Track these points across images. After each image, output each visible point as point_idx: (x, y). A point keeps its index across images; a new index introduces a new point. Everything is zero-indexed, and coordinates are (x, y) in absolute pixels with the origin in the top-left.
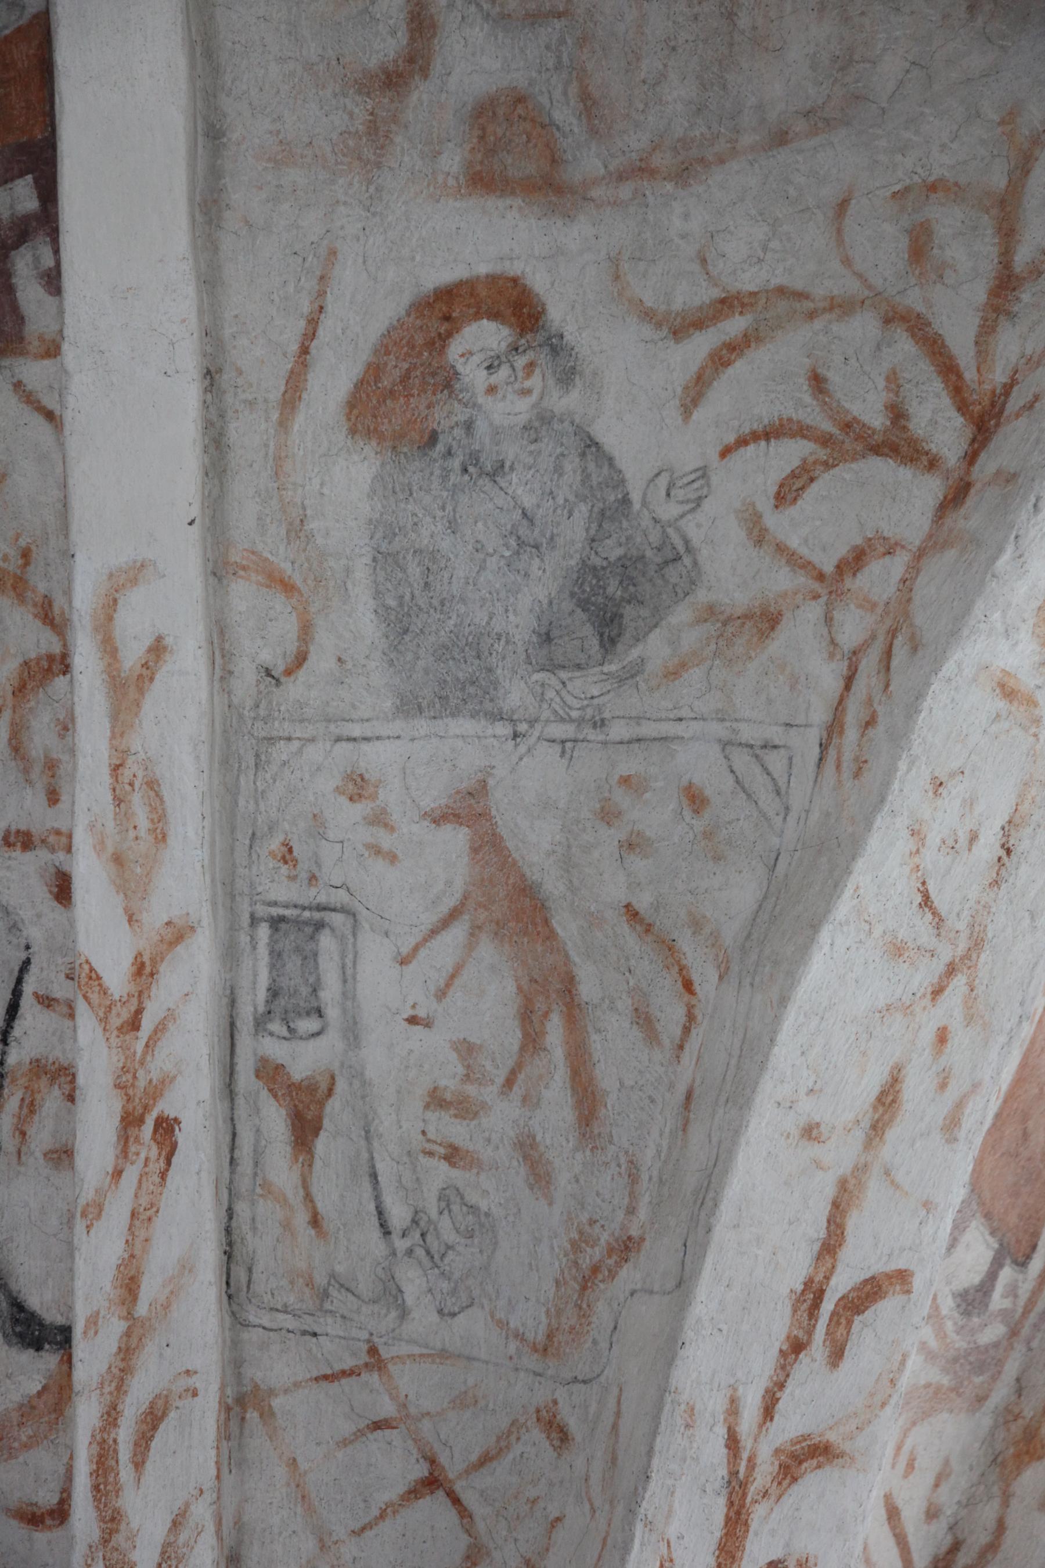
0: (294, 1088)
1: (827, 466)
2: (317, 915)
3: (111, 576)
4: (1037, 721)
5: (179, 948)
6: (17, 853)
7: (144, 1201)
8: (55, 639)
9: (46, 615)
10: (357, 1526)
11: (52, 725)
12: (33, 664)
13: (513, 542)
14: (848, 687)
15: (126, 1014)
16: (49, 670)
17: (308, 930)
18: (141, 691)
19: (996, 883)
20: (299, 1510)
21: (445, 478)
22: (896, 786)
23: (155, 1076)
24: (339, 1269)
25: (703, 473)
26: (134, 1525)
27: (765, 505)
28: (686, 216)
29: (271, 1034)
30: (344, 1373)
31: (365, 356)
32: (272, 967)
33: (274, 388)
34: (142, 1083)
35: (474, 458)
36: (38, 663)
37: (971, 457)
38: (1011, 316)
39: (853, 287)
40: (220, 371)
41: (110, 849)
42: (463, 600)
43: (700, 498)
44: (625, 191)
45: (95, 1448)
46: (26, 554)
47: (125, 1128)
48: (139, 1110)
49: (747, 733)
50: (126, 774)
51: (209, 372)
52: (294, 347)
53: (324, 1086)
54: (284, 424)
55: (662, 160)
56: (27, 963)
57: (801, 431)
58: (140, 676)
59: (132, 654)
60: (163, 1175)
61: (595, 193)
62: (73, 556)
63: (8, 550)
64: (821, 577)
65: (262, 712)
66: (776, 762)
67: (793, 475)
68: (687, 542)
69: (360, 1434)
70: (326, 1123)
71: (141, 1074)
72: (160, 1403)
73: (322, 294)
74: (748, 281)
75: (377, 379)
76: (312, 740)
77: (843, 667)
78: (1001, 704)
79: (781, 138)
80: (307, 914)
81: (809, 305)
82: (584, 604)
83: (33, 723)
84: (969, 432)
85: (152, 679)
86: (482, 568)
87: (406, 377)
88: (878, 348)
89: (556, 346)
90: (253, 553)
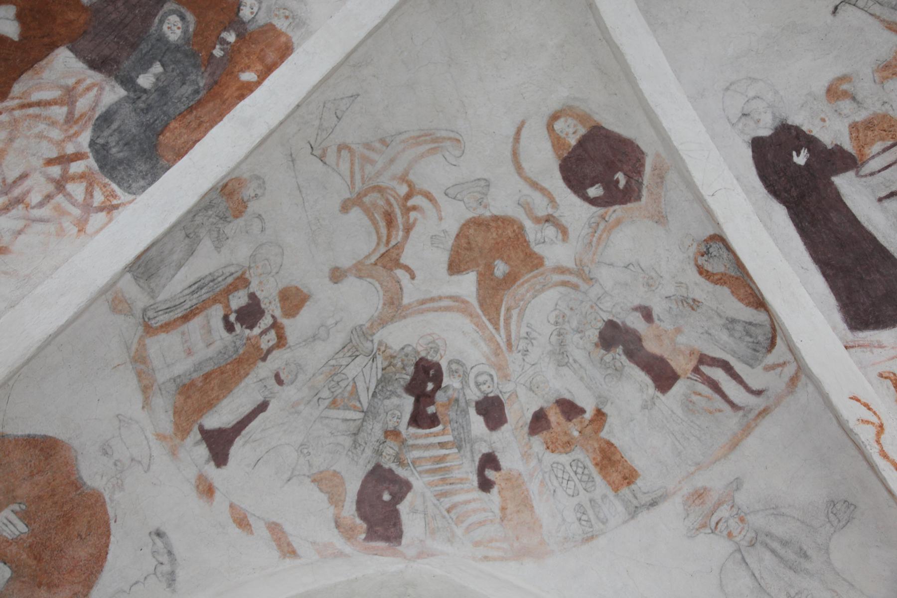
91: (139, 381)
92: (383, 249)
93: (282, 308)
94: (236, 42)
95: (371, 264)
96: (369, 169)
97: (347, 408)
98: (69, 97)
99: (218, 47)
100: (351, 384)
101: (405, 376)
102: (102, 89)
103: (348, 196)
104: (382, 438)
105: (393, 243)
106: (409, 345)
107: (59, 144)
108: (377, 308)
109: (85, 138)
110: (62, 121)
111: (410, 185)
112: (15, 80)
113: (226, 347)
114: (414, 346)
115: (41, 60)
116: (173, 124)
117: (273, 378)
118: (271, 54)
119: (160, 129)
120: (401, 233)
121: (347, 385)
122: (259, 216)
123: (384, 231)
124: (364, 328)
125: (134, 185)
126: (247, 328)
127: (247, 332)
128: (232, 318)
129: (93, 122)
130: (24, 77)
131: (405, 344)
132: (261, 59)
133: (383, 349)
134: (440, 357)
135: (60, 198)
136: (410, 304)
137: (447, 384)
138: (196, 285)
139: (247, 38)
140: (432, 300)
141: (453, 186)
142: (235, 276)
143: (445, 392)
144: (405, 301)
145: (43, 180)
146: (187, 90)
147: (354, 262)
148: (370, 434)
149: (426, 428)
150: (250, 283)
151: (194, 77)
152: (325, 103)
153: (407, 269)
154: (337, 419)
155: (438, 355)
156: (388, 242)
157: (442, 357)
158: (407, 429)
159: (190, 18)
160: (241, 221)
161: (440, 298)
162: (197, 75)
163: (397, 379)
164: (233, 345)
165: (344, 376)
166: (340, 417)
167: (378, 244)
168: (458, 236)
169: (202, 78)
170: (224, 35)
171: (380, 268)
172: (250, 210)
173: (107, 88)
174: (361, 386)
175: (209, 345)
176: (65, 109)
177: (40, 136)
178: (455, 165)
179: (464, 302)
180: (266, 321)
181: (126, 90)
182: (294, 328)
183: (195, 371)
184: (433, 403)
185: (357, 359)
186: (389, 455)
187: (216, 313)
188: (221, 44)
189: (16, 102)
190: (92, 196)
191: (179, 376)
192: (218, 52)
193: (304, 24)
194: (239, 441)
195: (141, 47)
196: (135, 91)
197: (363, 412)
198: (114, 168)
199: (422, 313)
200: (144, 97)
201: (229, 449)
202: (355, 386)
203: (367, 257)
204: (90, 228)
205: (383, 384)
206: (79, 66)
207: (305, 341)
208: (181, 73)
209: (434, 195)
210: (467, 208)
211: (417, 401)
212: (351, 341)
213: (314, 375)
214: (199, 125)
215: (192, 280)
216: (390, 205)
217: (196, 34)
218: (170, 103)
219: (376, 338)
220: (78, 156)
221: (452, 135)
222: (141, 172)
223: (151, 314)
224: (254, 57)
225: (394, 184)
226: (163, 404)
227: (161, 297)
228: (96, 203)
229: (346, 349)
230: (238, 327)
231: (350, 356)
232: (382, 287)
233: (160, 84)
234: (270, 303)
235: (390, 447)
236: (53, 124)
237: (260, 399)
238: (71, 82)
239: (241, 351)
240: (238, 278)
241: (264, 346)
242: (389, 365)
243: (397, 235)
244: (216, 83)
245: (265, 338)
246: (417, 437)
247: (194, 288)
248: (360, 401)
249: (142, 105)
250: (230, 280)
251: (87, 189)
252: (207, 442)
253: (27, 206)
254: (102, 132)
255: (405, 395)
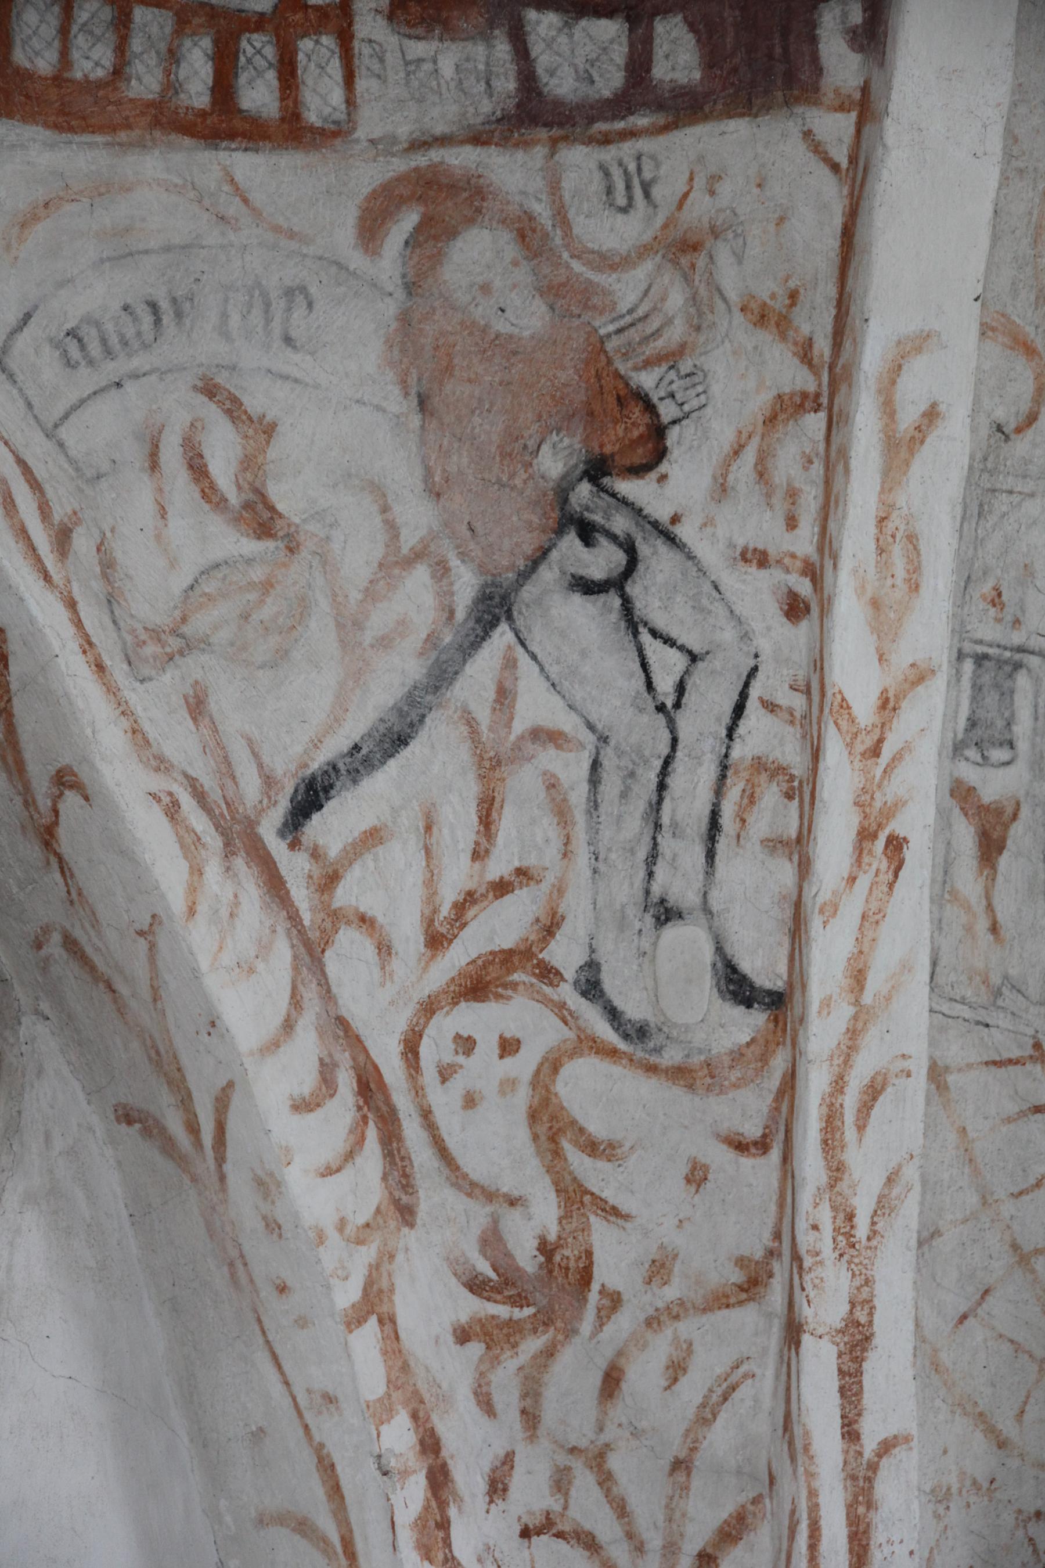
0: (983, 809)
2: (1018, 657)
3: (899, 342)
5: (920, 689)
6: (753, 569)
7: (874, 906)
8: (811, 378)
9: (805, 355)
10: (1016, 1190)
11: (798, 457)
12: (786, 398)
15: (869, 741)
16: (801, 406)
17: (1008, 669)
18: (912, 452)
20: (967, 1170)
23: (890, 799)
24: (1013, 972)
26: (856, 1176)
29: (967, 759)
30: (1010, 1062)
32: (974, 699)
34: (878, 804)
36: (791, 398)
41: (869, 594)
45: (825, 1110)
46: (793, 296)
47: (860, 841)
48: (874, 827)
50: (890, 526)
53: (1009, 811)
56: (755, 669)
58: (913, 438)
59: (908, 417)
60: (891, 886)
62: (866, 320)
63: (776, 289)
65: (990, 465)
69: (1022, 1114)
70: (1009, 843)
71: (878, 795)
72: (880, 1078)
76: (1032, 495)
80: (1008, 654)
83: (780, 452)
85: (922, 442)
90: (1003, 315)
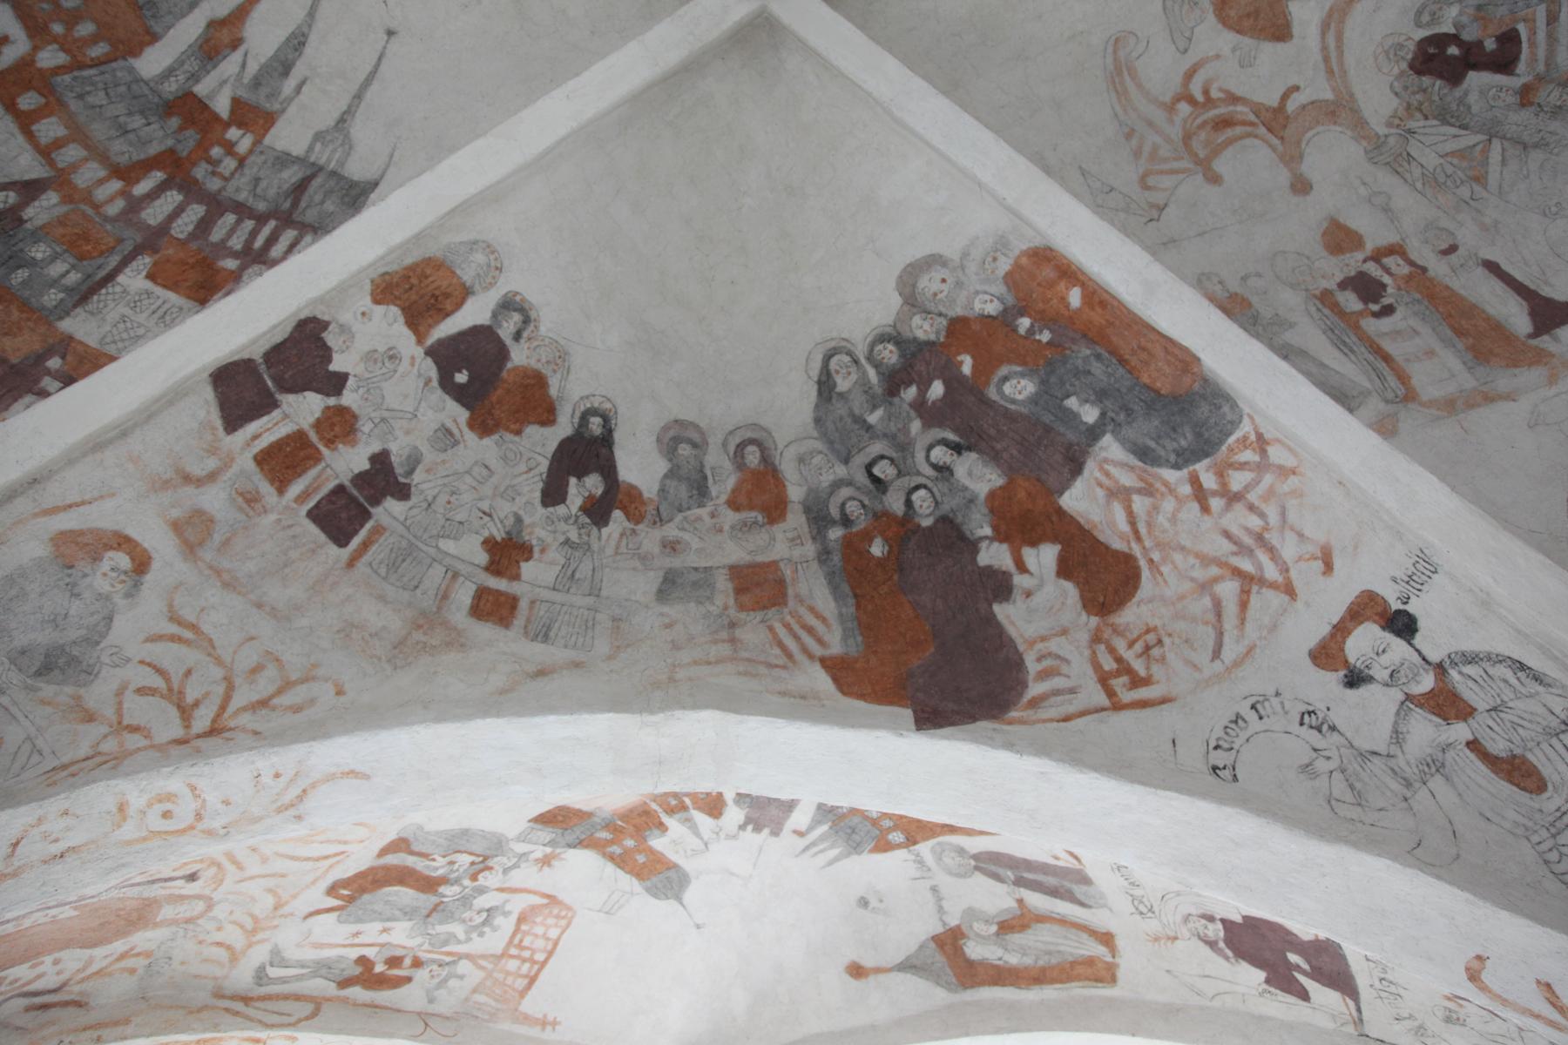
1: (162, 696)
4: (119, 826)
13: (52, 618)
14: (84, 760)
19: (45, 862)
21: (59, 580)
22: (52, 800)
25: (128, 660)
27: (132, 687)
28: (213, 595)
31: (84, 527)
33: (48, 503)
35: (75, 585)
37: (199, 736)
38: (254, 712)
39: (228, 660)
40: (39, 483)
42: (15, 615)
43: (118, 666)
44: (207, 572)
49: (40, 742)
51: (35, 480)
52: (68, 502)
54: (36, 515)
55: (225, 576)
57: (167, 679)
61: (199, 563)
64: (120, 723)
66: (36, 758)
67: (150, 689)
68: (99, 673)
73: (96, 500)
74: (206, 628)
75: (79, 536)
77: (91, 753)
78: (115, 810)
79: (259, 606)
81: (212, 652)
82: (47, 656)
84: (207, 729)
86: (34, 614)
87: (87, 544)
88: (215, 682)
89: (137, 585)
91: (1479, 406)
92: (1262, 130)
93: (1352, 251)
94: (1030, 317)
95: (1283, 143)
96: (1164, 152)
97: (1485, 162)
98: (1120, 494)
99: (1038, 337)
100: (1449, 159)
101: (1437, 87)
102: (1106, 460)
103: (1200, 177)
104: (1532, 109)
105: (1252, 118)
106: (1391, 86)
107: (1180, 501)
108: (1341, 132)
109: (1170, 475)
110: (1151, 500)
111: (1178, 99)
112: (1107, 548)
113: (1416, 314)
114: (1392, 78)
115: (1078, 523)
116: (1145, 379)
117: (1449, 257)
118: (1044, 274)
119: (1153, 394)
120: (1239, 108)
121: (1451, 164)
122: (1244, 279)
123: (1239, 130)
124: (1369, 148)
125: (1229, 417)
126: (1385, 291)
127: (1390, 290)
128: (1375, 307)
129: (1149, 468)
130: (1101, 538)
131: (1388, 91)
132: (1051, 285)
133: (1397, 121)
134: (1411, 41)
135: (1252, 497)
136: (1333, 90)
137: (1451, 25)
138: (1342, 348)
139: (1024, 303)
140: (1326, 59)
141: (1174, 43)
142: (1320, 306)
143: (1463, 27)
144: (1329, 95)
145: (1229, 515)
146: (1097, 368)
147: (1281, 165)
148: (1526, 126)
149: (1521, 48)
150: (1326, 289)
151: (1080, 361)
152: (1098, 206)
153: (1285, 97)
154: (1502, 172)
155: (1406, 43)
156: (1252, 124)
157: (1410, 38)
158: (1518, 75)
159: (1004, 370)
160: (1254, 300)
161: (1324, 48)
162: (1077, 358)
163: (1441, 99)
164: (1410, 305)
165: (1438, 170)
166: (1499, 169)
167: (1256, 136)
168: (1238, 32)
169: (1079, 352)
170: (1022, 331)
171: (1287, 133)
172: (1238, 290)
173: (1104, 454)
174: (1451, 146)
175: (1416, 332)
176: (1136, 498)
177: (1173, 519)
178: (1148, 42)
179: (1330, 15)
180: (1372, 269)
181: (1104, 436)
182: (1376, 233)
183: (1454, 346)
184: (1479, 44)
185: (1412, 154)
186: (1561, 96)
187: (1371, 325)
188: (1034, 334)
189: (1134, 545)
190: (1246, 463)
191: (1464, 363)
192: (1045, 337)
193: (1002, 237)
194: (1546, 291)
195: (1048, 421)
196: (1105, 425)
197: (1490, 140)
198: (1207, 442)
199: (1345, 72)
200: (1110, 414)
201: (1559, 302)
202: (1452, 154)
203: (1274, 149)
204: (1290, 462)
205: (1448, 117)
206: (1079, 486)
207: (1392, 221)
208: (1075, 376)
209: (1188, 67)
210: (1202, 21)
211: (1476, 67)
212: (1388, 163)
213: (1439, 208)
214: (1144, 349)
215: (1337, 353)
216: (1205, 123)
217: (1024, 363)
218: (1116, 386)
219: (1382, 130)
220: (1195, 481)
221: (1110, 50)
222: (1211, 411)
223: (1390, 395)
224: (1049, 294)
225: (1178, 120)
226: (1504, 380)
227: (1367, 384)
228: (1257, 458)
229: (1399, 169)
230: (1386, 301)
231: (1409, 163)
232: (1311, 128)
233: (1093, 398)
234: (1347, 265)
235: (1548, 96)
236: (1156, 508)
237: (1480, 272)
238: (1100, 493)
239: (1417, 296)
240: (1323, 303)
241: (1406, 270)
242: (1420, 110)
243: (1241, 113)
244: (1085, 336)
245: (1394, 269)
246: (1533, 59)
247: (1346, 351)
248: (1474, 146)
249: (1122, 416)
250: (1326, 311)
251: (1237, 469)
252: (1552, 329)
253: (1266, 528)
254: (1160, 457)
255: (1465, 85)
